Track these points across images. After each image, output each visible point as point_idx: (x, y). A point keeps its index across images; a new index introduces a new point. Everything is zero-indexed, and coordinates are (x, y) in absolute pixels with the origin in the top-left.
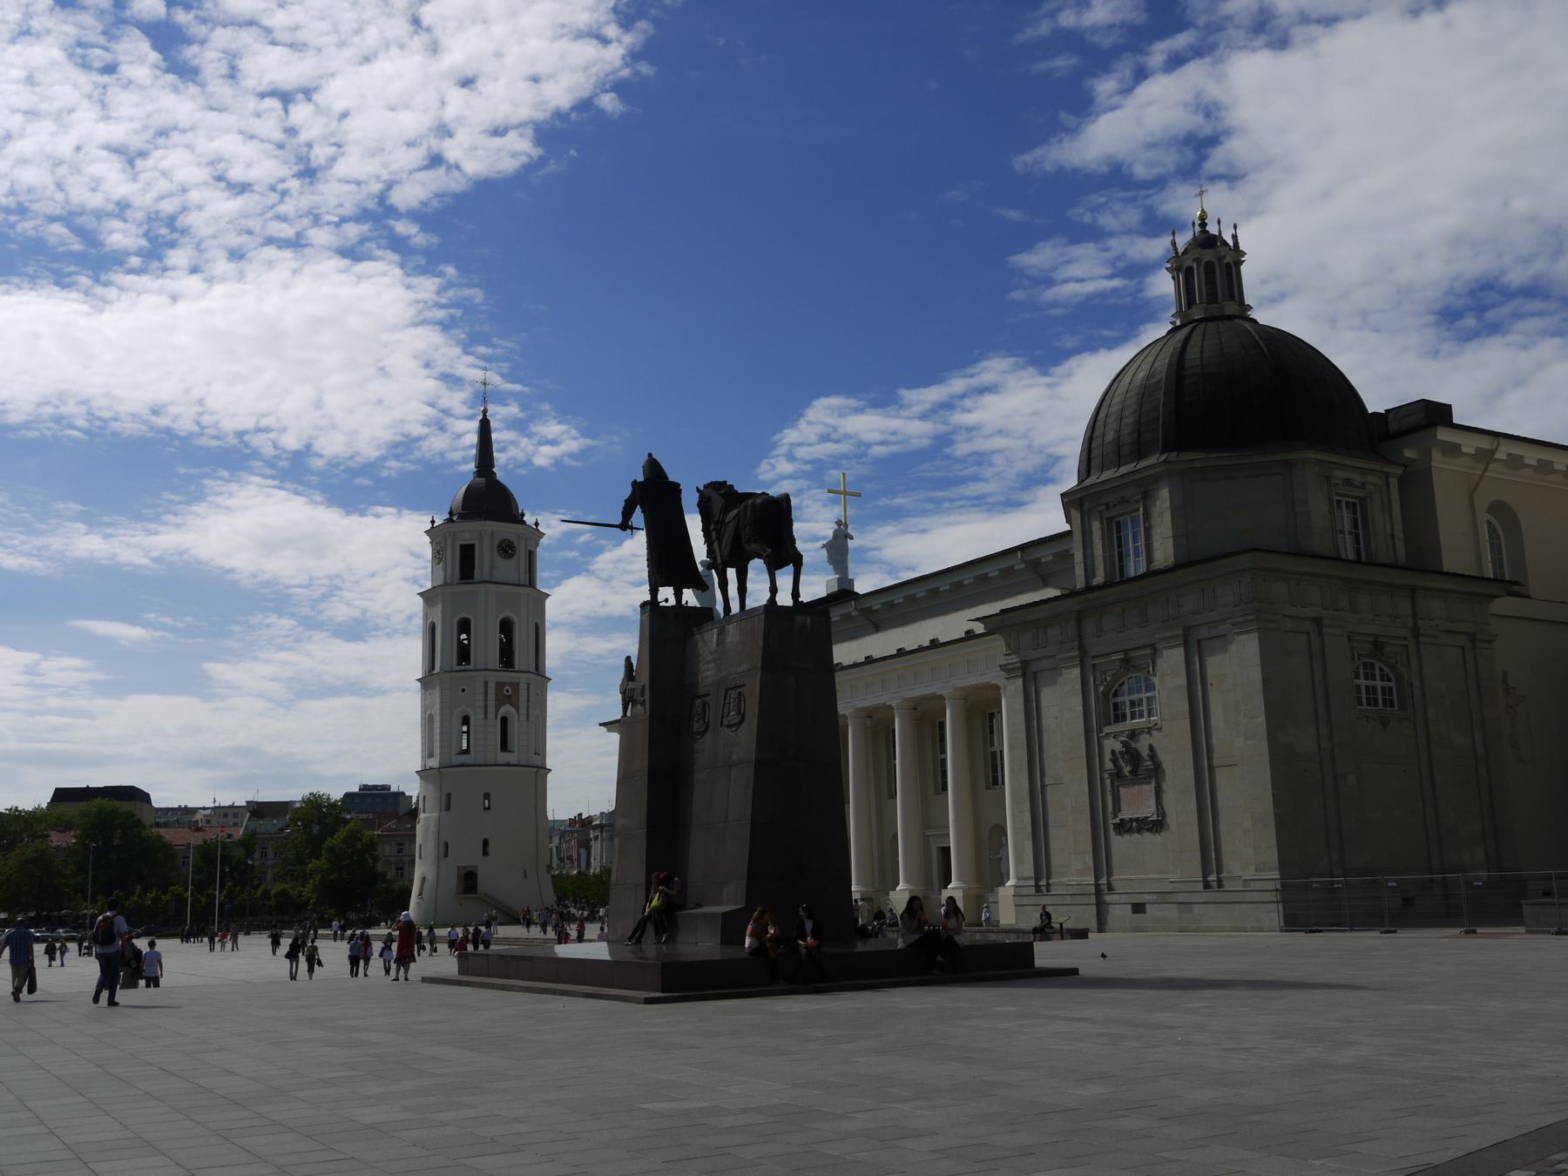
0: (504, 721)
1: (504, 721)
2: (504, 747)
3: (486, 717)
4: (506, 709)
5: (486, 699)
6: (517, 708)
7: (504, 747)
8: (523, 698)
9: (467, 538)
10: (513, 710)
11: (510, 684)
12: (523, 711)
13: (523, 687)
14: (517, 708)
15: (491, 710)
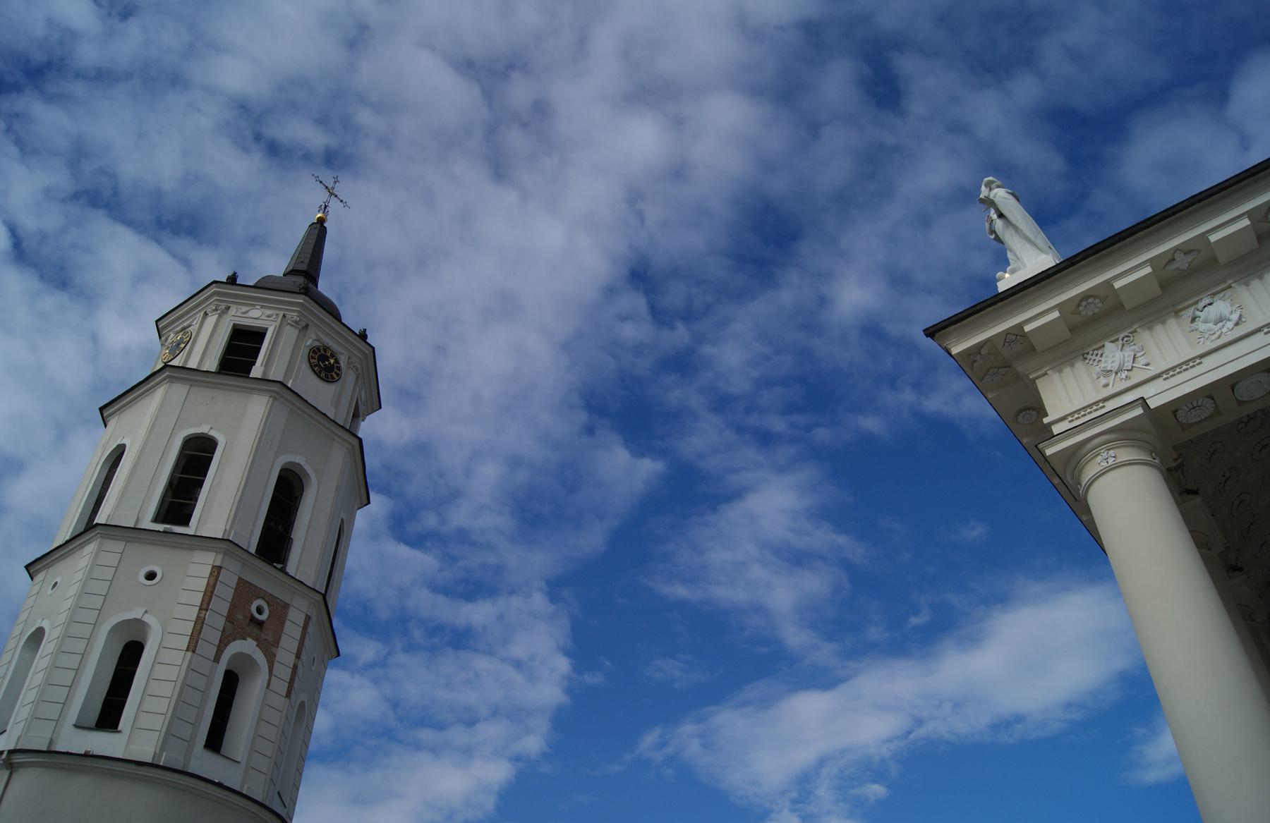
0: (231, 683)
1: (231, 683)
2: (215, 741)
3: (192, 647)
4: (247, 646)
5: (204, 607)
6: (271, 659)
7: (215, 741)
8: (288, 643)
9: (254, 316)
10: (260, 657)
11: (270, 599)
12: (283, 671)
13: (295, 617)
14: (271, 659)
15: (212, 635)
